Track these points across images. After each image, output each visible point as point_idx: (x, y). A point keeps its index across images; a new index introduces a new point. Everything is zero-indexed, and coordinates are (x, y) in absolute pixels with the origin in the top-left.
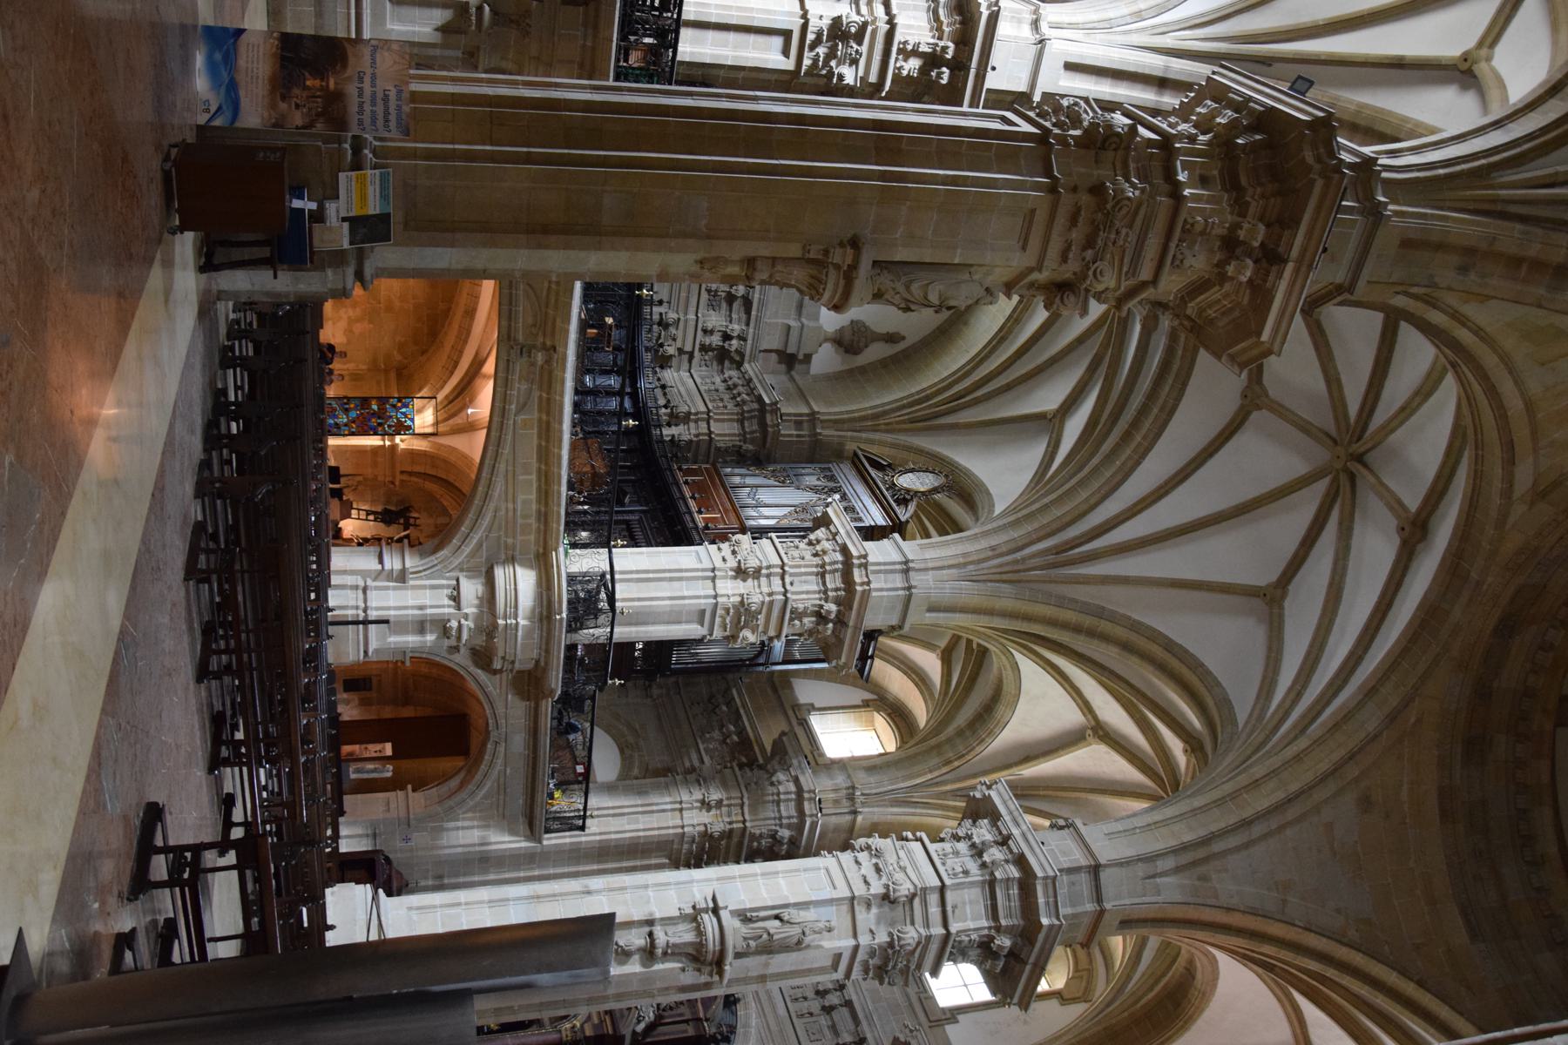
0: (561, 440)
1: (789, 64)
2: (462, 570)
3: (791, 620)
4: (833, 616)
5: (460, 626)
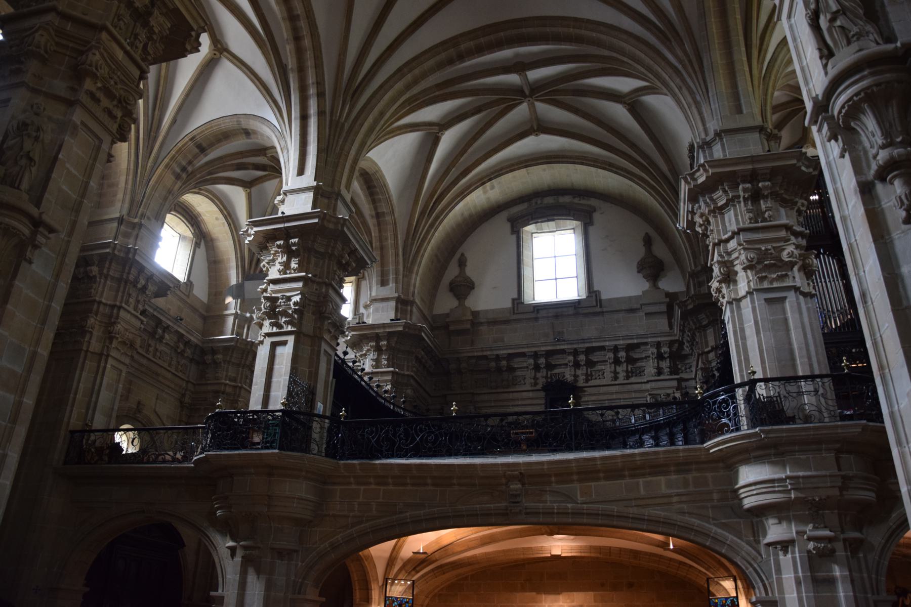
0: (585, 459)
1: (291, 339)
2: (758, 542)
3: (764, 220)
4: (748, 185)
5: (810, 539)
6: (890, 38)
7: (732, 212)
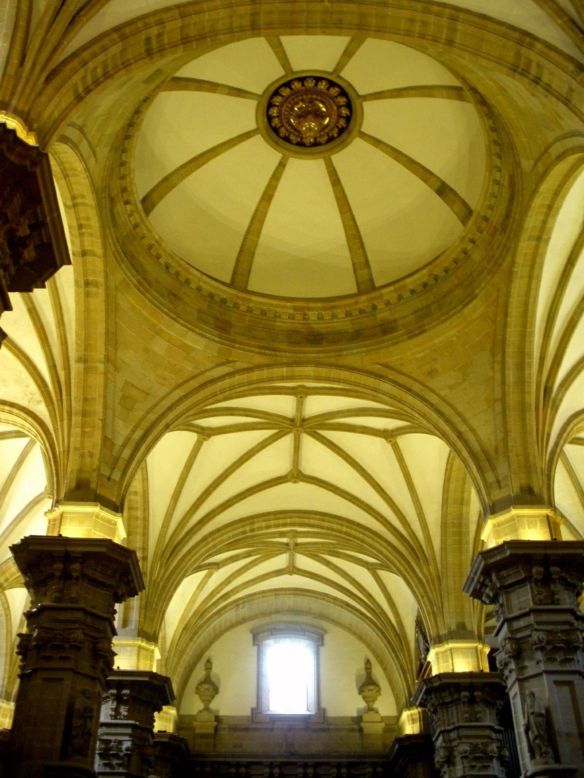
3: (477, 720)
6: (557, 759)
7: (454, 707)
